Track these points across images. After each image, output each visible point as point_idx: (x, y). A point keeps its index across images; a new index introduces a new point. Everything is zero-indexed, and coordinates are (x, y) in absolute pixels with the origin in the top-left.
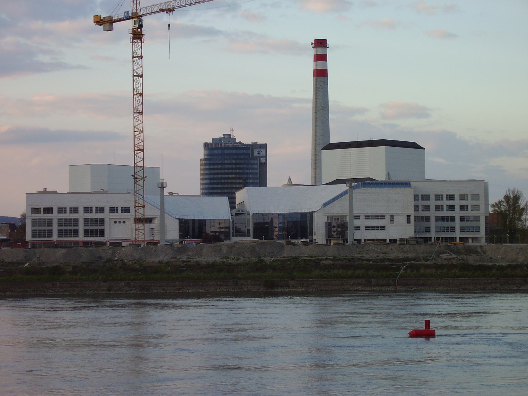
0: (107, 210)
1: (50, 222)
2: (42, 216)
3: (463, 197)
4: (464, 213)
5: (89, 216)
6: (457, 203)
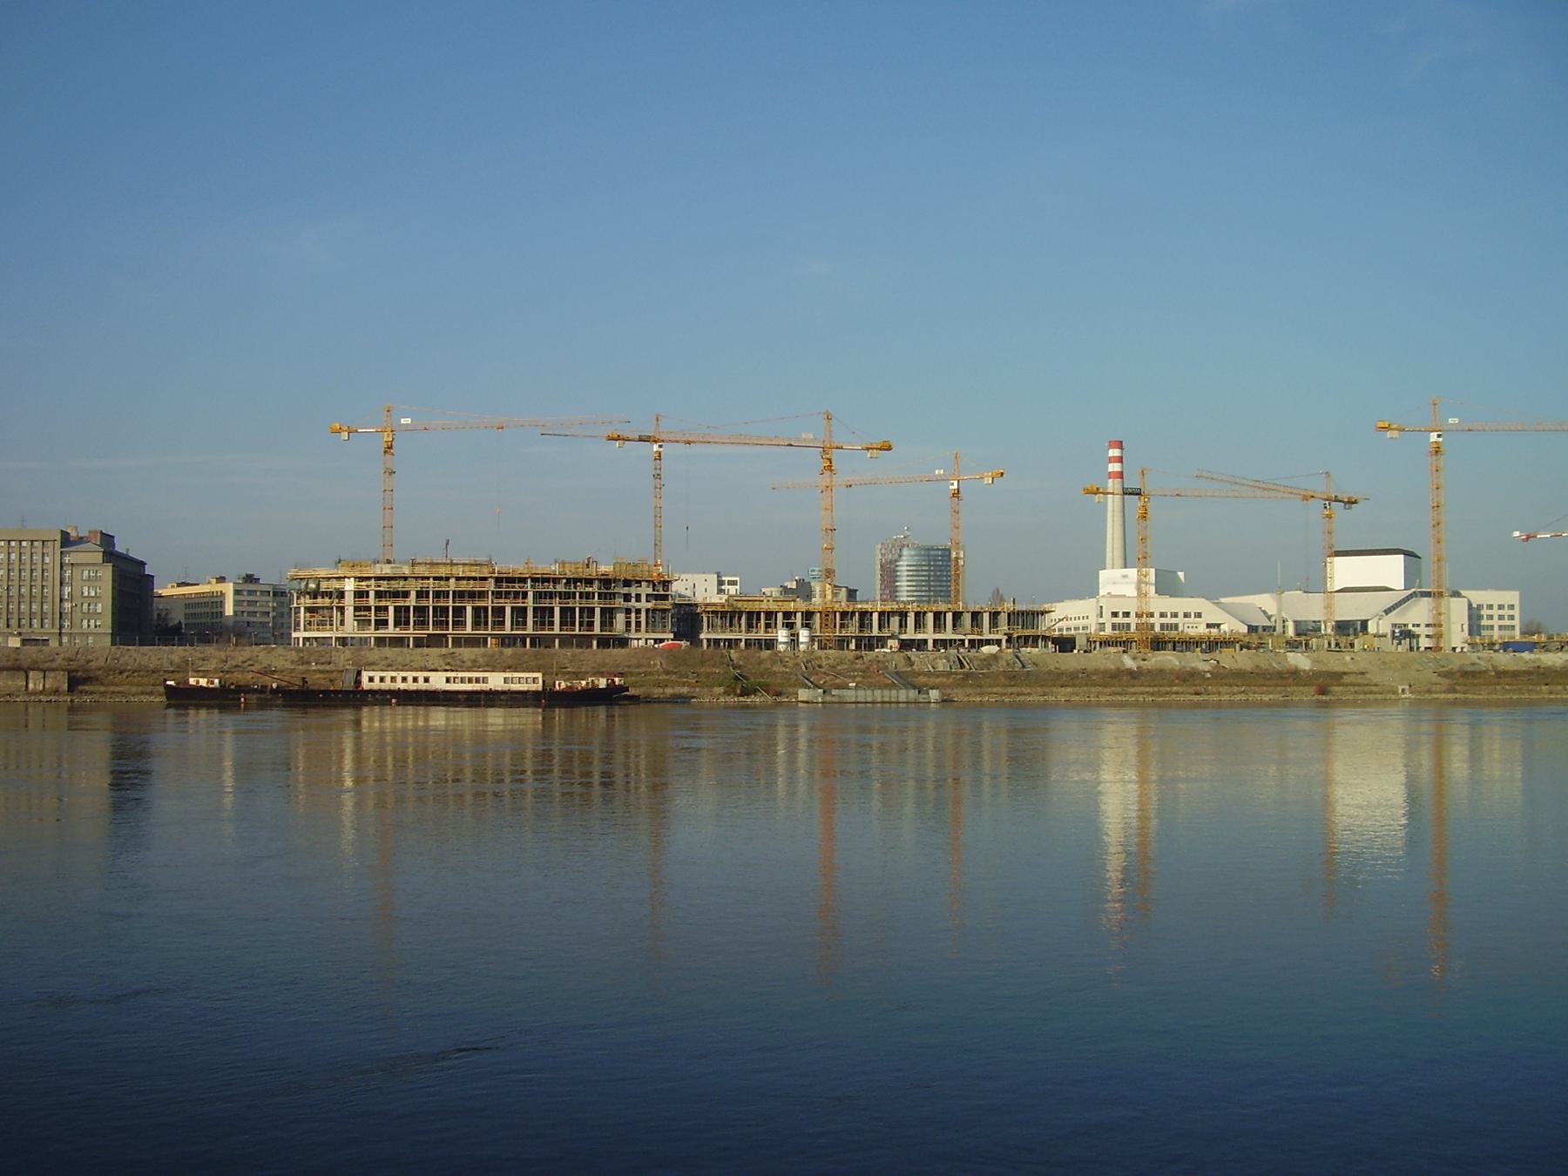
0: (1181, 615)
1: (1128, 625)
2: (1120, 620)
3: (1501, 607)
4: (1502, 623)
5: (1164, 620)
6: (1495, 612)
